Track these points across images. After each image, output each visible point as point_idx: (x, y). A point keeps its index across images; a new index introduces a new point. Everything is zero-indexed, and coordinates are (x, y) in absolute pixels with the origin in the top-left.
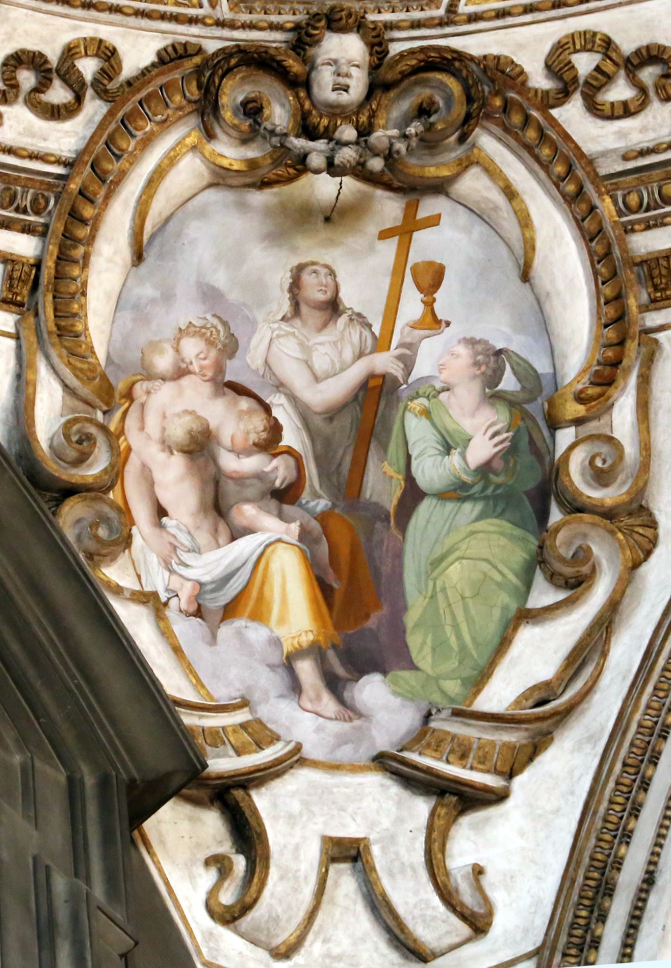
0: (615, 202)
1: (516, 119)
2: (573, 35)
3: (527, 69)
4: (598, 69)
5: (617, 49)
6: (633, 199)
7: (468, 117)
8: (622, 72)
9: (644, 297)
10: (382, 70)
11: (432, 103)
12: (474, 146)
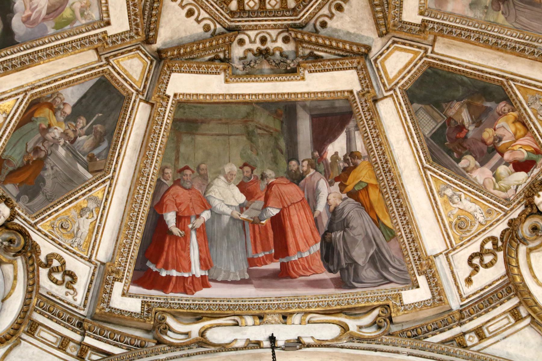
0: (37, 301)
1: (30, 262)
2: (58, 255)
3: (42, 253)
4: (57, 267)
5: (65, 266)
6: (42, 304)
7: (20, 252)
8: (62, 273)
9: (26, 329)
10: (9, 223)
11: (14, 241)
12: (16, 260)
